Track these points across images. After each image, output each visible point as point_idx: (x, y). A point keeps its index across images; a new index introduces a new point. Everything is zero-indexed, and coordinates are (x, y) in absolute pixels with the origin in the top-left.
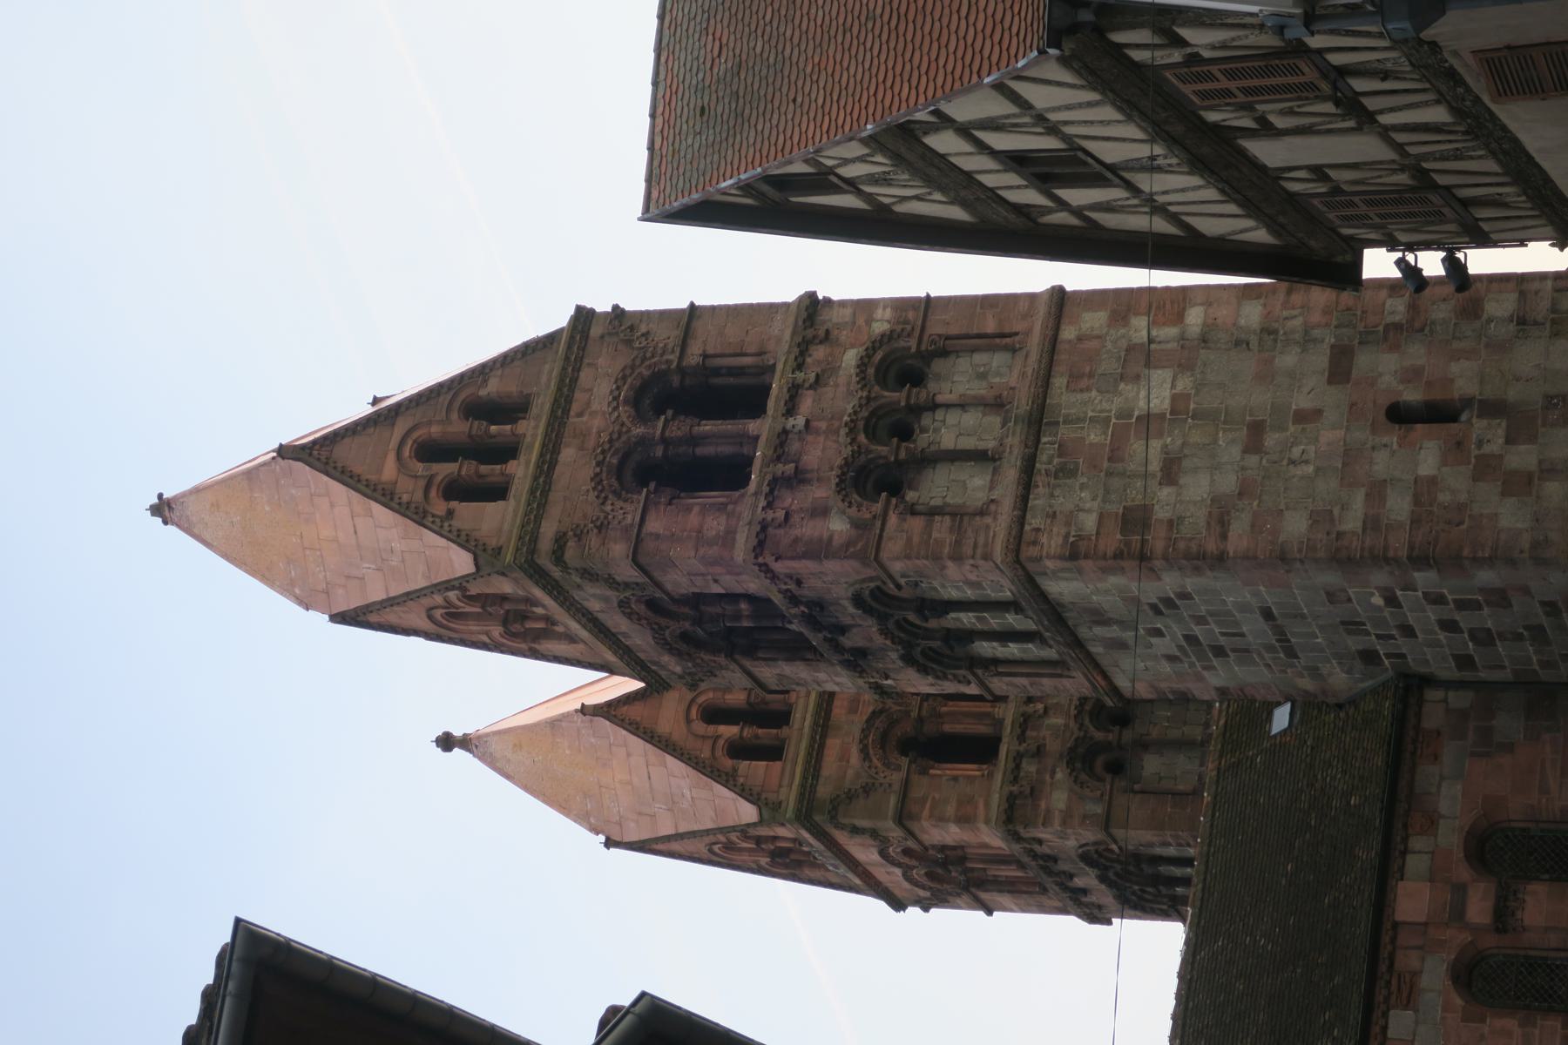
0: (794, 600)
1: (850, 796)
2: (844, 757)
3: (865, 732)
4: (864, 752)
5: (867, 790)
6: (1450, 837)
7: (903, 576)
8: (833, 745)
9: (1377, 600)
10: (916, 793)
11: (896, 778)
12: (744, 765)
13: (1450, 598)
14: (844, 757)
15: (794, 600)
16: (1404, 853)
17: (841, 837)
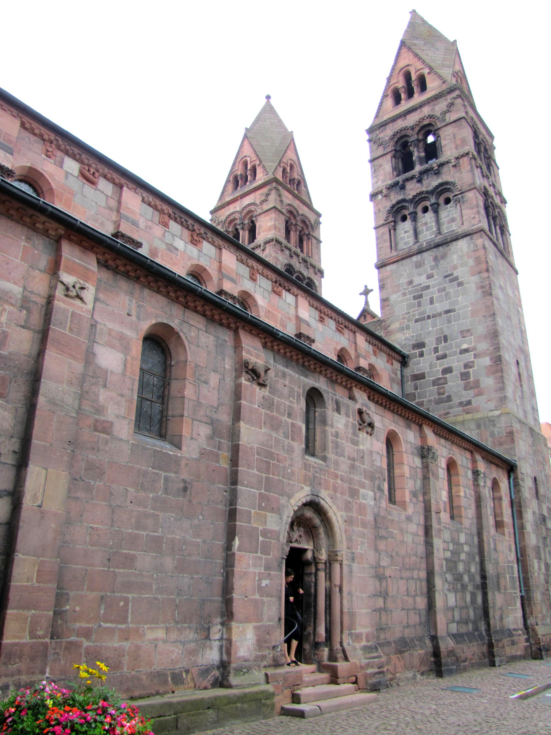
0: (441, 165)
1: (280, 196)
2: (287, 198)
3: (294, 207)
4: (289, 205)
5: (281, 201)
6: (373, 360)
7: (462, 197)
8: (290, 196)
9: (465, 346)
10: (281, 215)
11: (284, 211)
12: (282, 169)
13: (471, 370)
14: (287, 198)
15: (441, 165)
16: (369, 342)
17: (265, 190)
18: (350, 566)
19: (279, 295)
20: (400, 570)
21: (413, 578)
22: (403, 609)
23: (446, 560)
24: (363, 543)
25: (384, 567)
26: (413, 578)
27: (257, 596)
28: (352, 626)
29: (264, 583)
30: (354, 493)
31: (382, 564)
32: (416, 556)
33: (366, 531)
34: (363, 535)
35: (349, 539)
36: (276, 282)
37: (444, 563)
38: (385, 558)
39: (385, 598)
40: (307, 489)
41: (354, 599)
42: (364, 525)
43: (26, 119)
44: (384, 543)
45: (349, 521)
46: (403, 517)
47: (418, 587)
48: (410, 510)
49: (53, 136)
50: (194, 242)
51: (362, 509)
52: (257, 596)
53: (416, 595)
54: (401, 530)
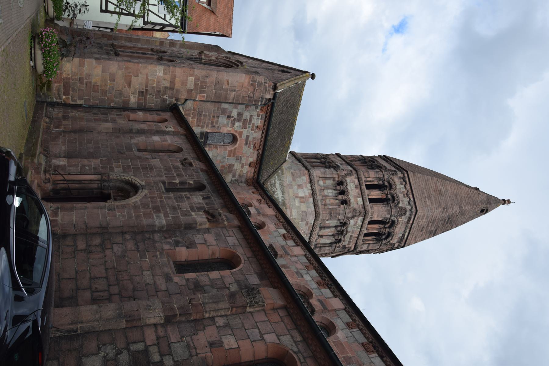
18: (104, 207)
19: (367, 350)
20: (114, 268)
21: (109, 285)
22: (77, 272)
23: (146, 351)
24: (124, 216)
25: (112, 248)
26: (109, 285)
27: (80, 165)
28: (63, 209)
29: (87, 168)
30: (157, 210)
31: (114, 246)
32: (134, 290)
33: (134, 218)
34: (130, 217)
35: (123, 207)
36: (371, 342)
37: (140, 346)
38: (120, 250)
39: (85, 250)
40: (143, 183)
41: (82, 211)
42: (137, 217)
43: (278, 214)
44: (133, 248)
45: (135, 207)
46: (167, 270)
47: (101, 294)
48: (177, 279)
49: (283, 221)
50: (318, 283)
51: (148, 215)
52: (80, 165)
53: (92, 292)
54: (152, 268)
